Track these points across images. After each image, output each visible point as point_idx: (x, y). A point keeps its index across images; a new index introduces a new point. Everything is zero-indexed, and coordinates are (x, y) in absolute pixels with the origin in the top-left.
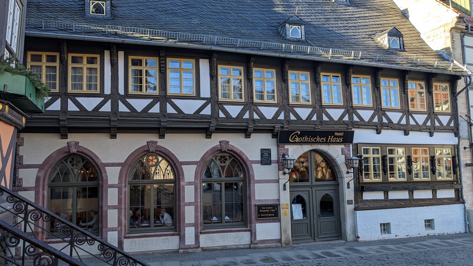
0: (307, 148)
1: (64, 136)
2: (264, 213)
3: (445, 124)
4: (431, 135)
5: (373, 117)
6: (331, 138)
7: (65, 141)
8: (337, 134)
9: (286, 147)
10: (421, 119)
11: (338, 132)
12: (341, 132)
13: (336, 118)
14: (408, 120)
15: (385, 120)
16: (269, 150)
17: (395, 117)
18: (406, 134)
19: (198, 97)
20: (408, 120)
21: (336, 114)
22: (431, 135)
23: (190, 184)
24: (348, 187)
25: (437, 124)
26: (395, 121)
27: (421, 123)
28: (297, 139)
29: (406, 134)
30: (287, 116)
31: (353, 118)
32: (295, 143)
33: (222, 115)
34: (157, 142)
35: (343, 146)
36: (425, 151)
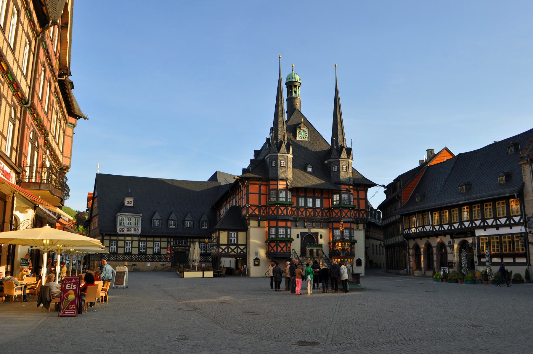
0: (461, 240)
1: (414, 240)
2: (450, 265)
3: (517, 221)
4: (511, 228)
5: (481, 223)
6: (467, 235)
7: (415, 241)
8: (468, 233)
9: (454, 240)
10: (503, 221)
11: (468, 232)
12: (469, 232)
13: (467, 226)
14: (496, 222)
15: (474, 225)
16: (450, 241)
17: (490, 222)
18: (497, 229)
19: (429, 225)
20: (496, 222)
21: (467, 224)
22: (511, 228)
23: (435, 254)
24: (475, 256)
25: (512, 222)
26: (490, 224)
27: (503, 223)
28: (456, 236)
29: (497, 229)
30: (451, 228)
31: (485, 224)
32: (456, 238)
33: (434, 230)
34: (428, 240)
35: (473, 238)
36: (486, 238)
